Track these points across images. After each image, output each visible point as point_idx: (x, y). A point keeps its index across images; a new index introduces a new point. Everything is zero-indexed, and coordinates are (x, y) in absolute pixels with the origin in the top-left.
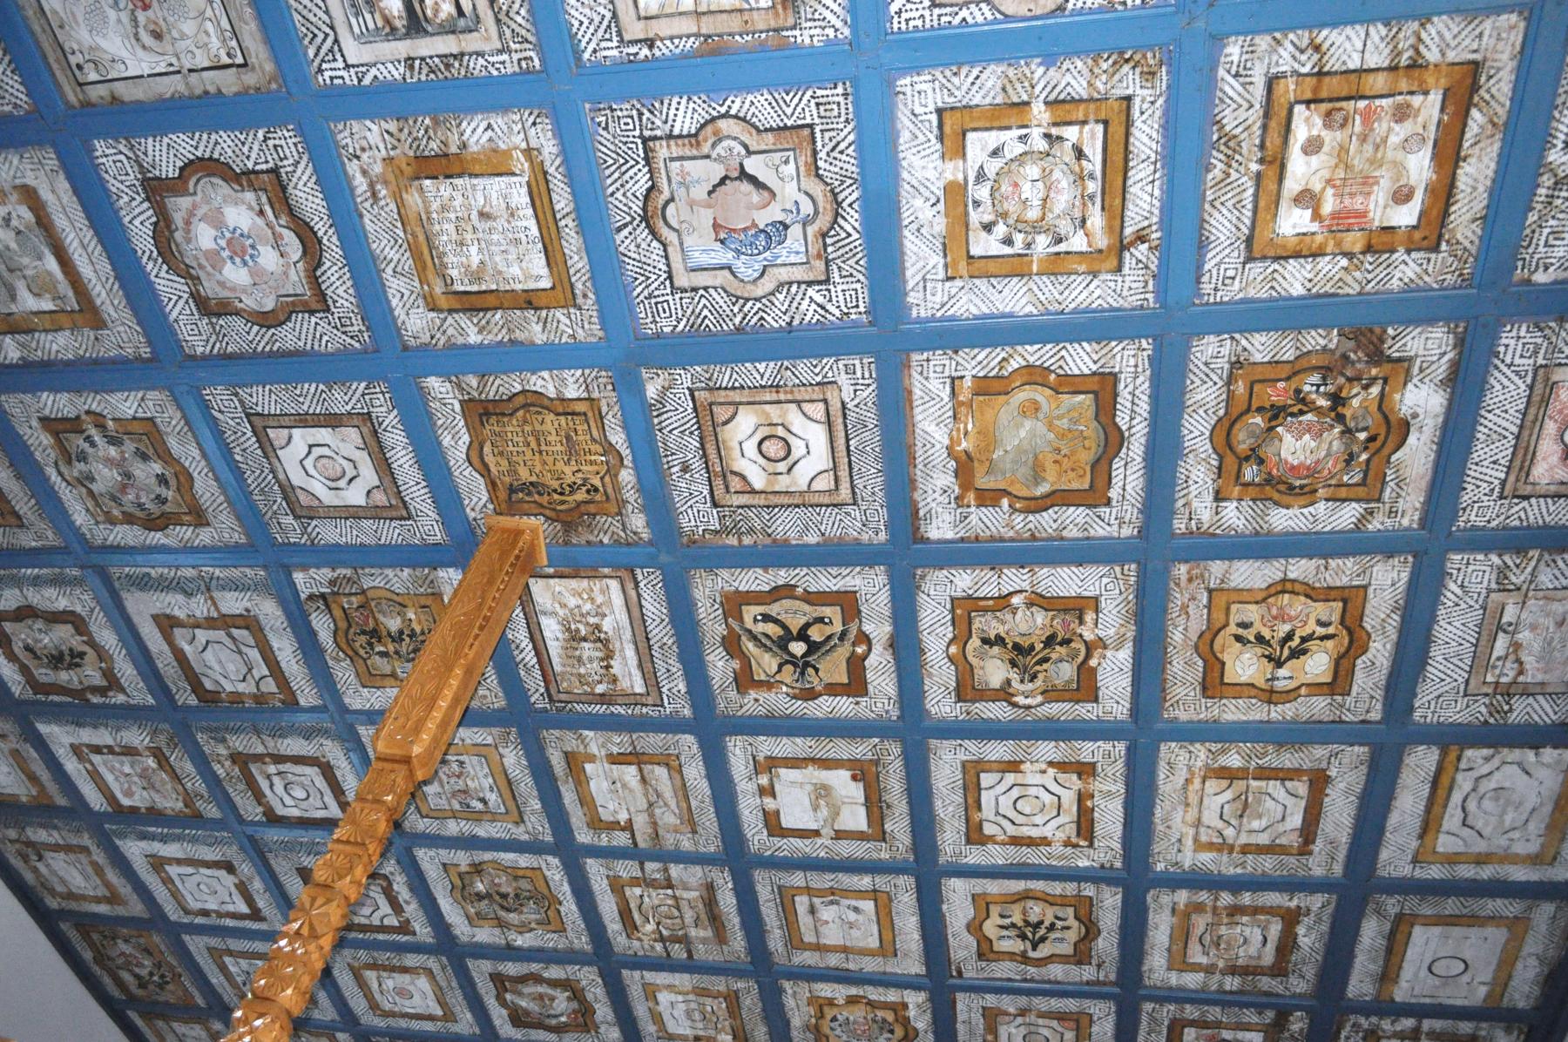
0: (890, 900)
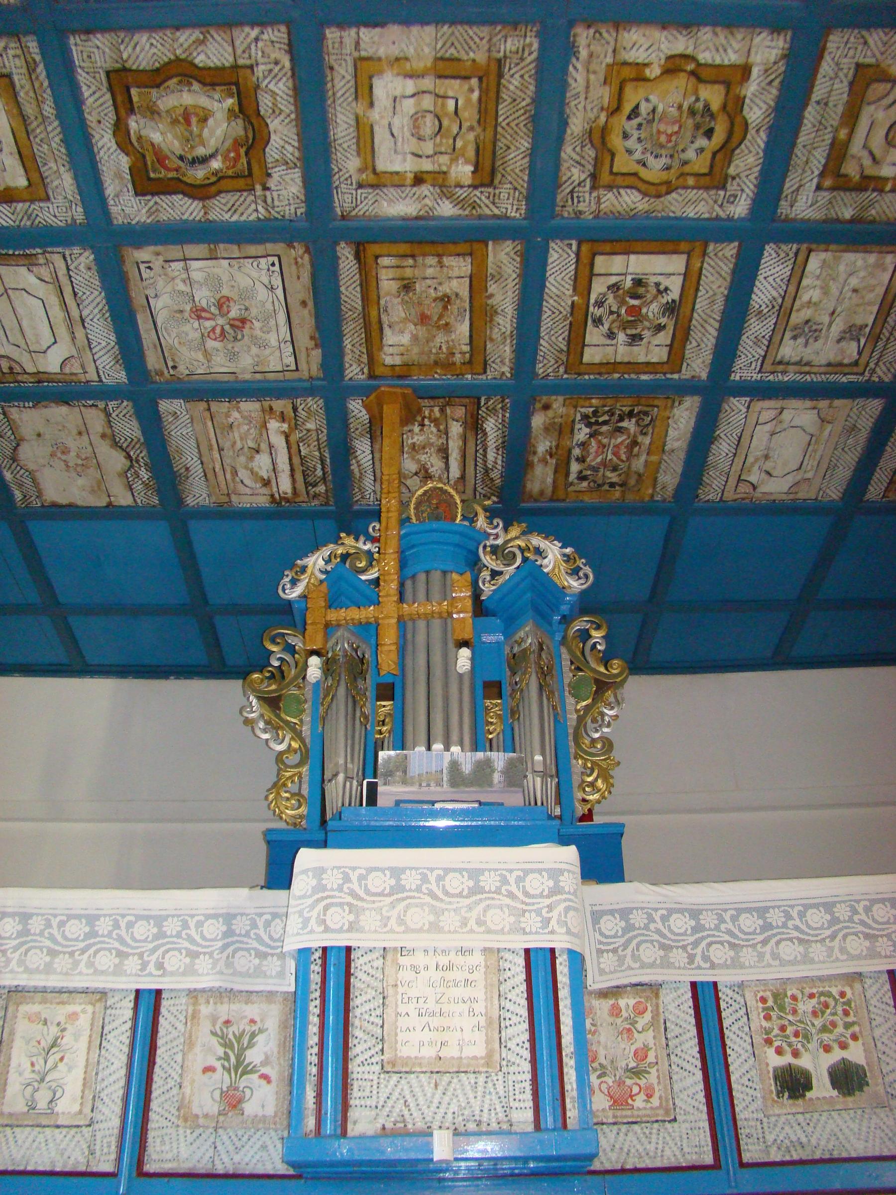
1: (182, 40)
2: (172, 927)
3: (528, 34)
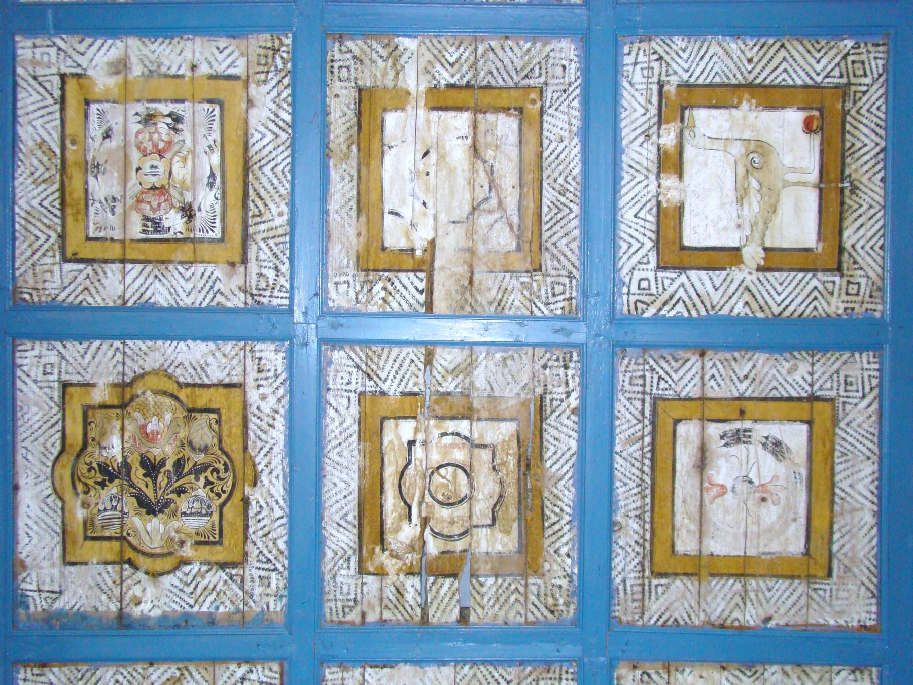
0: (835, 421)
1: (154, 678)
3: (564, 676)
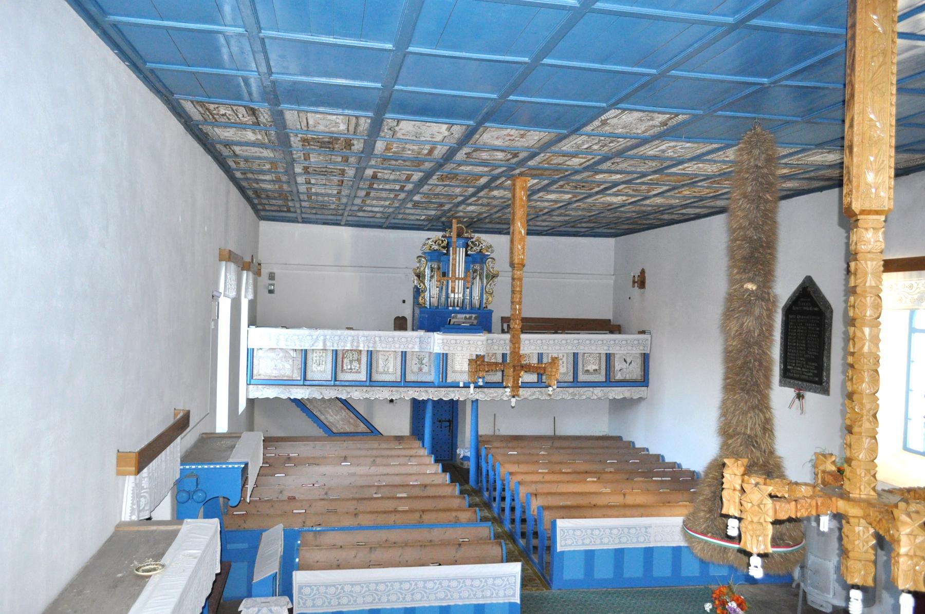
2: (409, 339)
